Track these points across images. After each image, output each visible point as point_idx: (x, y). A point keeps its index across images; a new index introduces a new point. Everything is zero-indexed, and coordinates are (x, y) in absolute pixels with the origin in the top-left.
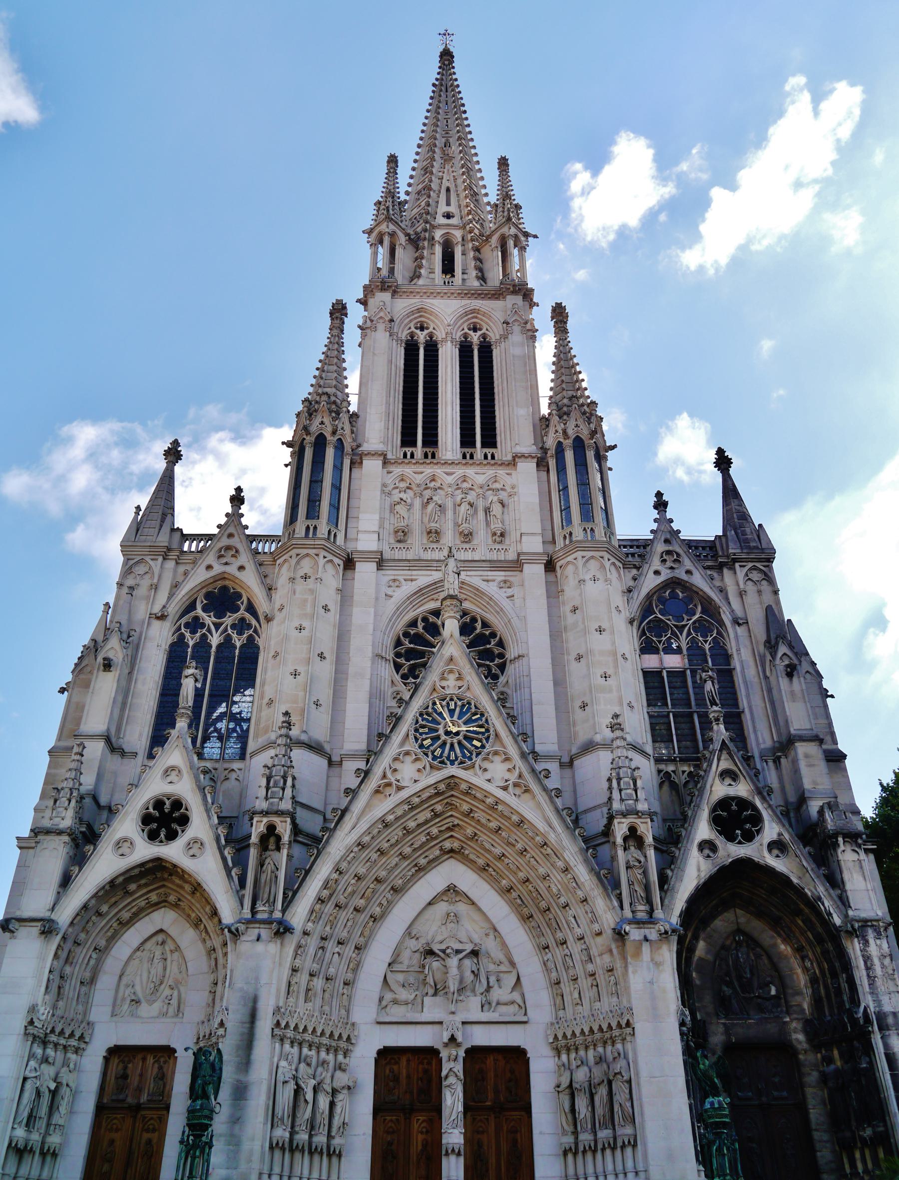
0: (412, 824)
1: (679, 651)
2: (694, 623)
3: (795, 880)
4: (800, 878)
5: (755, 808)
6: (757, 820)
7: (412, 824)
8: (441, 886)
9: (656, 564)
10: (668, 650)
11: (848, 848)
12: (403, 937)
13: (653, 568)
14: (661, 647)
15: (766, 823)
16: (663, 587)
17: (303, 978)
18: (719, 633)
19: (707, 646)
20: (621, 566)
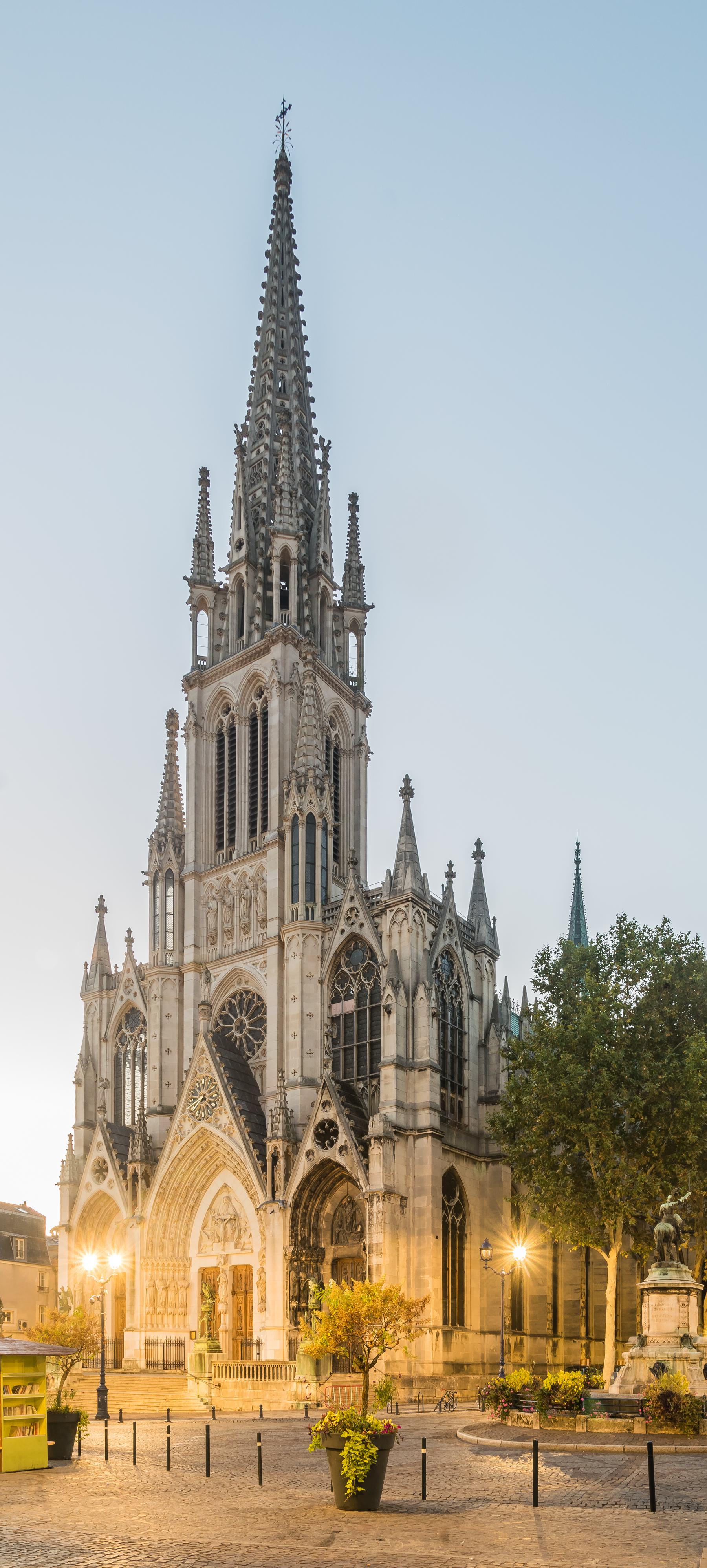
0: (193, 1157)
1: (351, 997)
2: (364, 969)
3: (348, 1170)
4: (351, 1168)
5: (337, 1126)
6: (336, 1133)
7: (193, 1157)
8: (220, 1185)
9: (342, 924)
10: (348, 997)
11: (376, 1146)
12: (207, 1213)
13: (340, 928)
14: (342, 995)
15: (340, 1134)
16: (348, 942)
17: (156, 1242)
18: (378, 976)
19: (368, 988)
20: (319, 933)
